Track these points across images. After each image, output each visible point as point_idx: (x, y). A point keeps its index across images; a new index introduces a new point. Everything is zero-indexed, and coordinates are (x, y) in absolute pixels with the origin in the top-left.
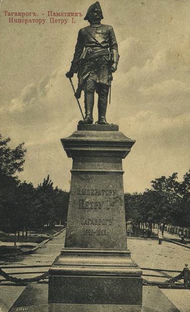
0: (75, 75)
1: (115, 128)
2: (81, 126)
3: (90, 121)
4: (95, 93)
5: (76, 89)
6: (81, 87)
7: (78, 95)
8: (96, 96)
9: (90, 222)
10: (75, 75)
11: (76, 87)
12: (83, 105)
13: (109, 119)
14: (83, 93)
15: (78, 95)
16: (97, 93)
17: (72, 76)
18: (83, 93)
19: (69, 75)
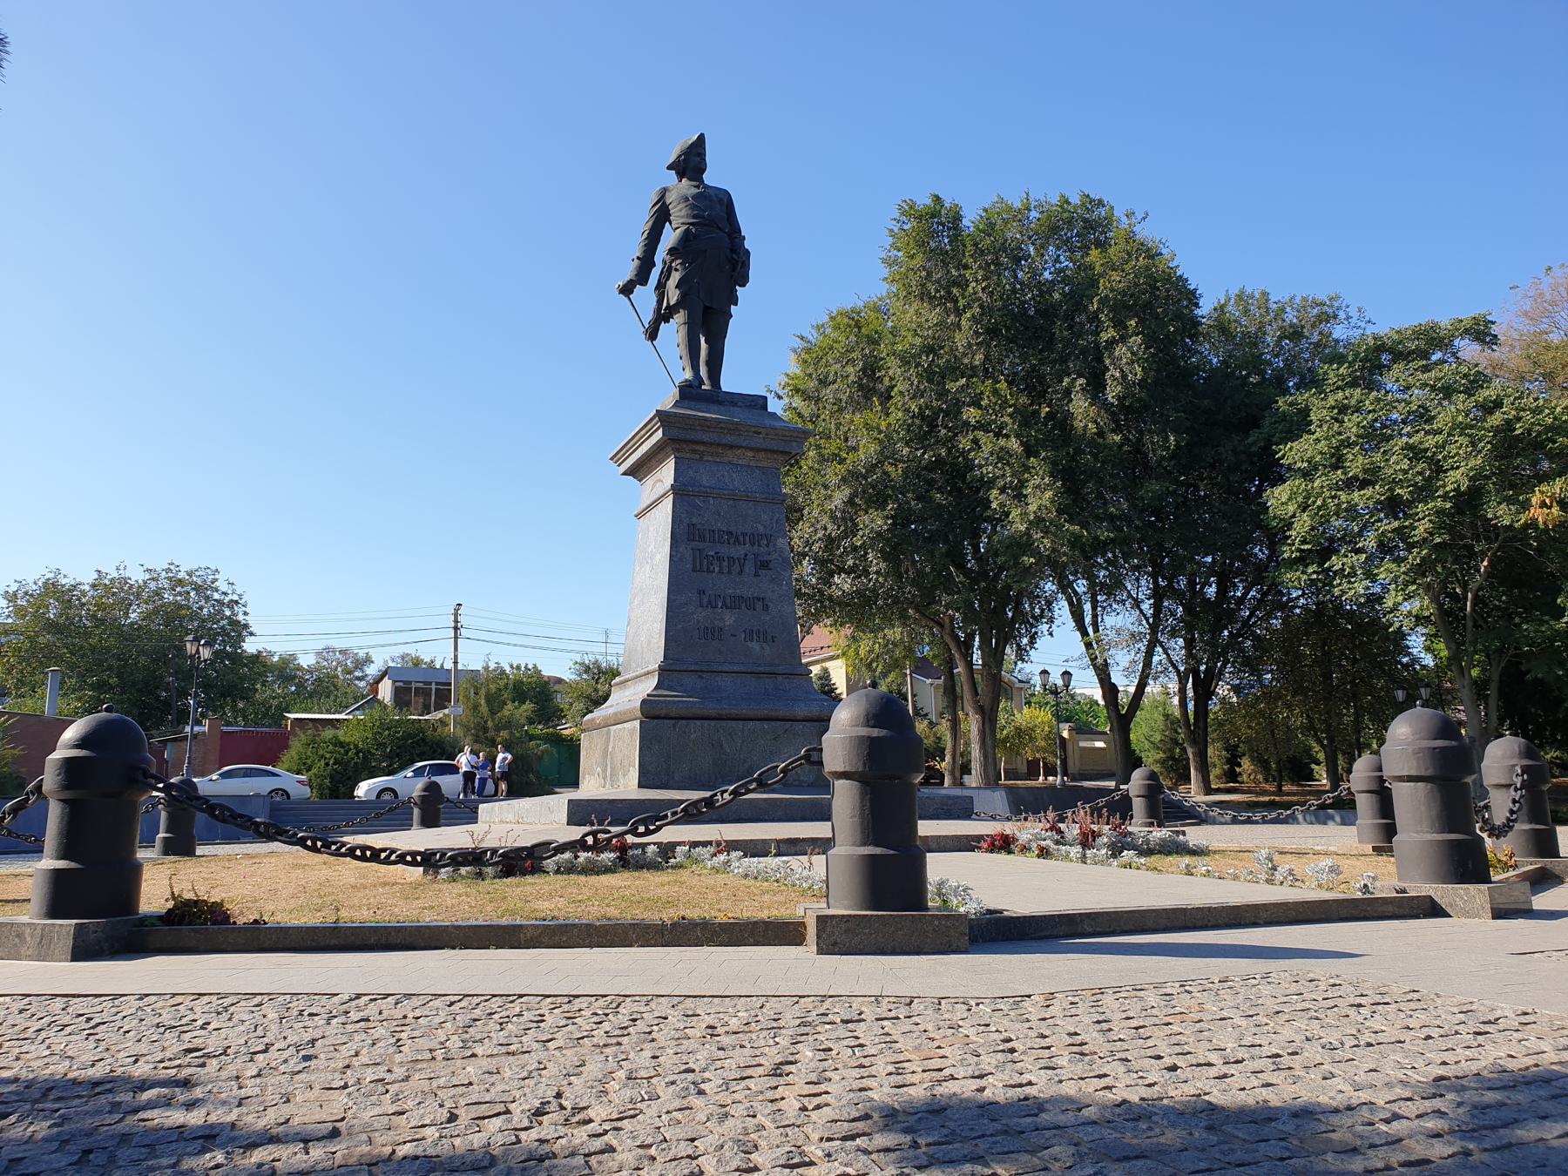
6: (663, 316)
9: (720, 605)
11: (648, 316)
15: (652, 334)
19: (627, 290)
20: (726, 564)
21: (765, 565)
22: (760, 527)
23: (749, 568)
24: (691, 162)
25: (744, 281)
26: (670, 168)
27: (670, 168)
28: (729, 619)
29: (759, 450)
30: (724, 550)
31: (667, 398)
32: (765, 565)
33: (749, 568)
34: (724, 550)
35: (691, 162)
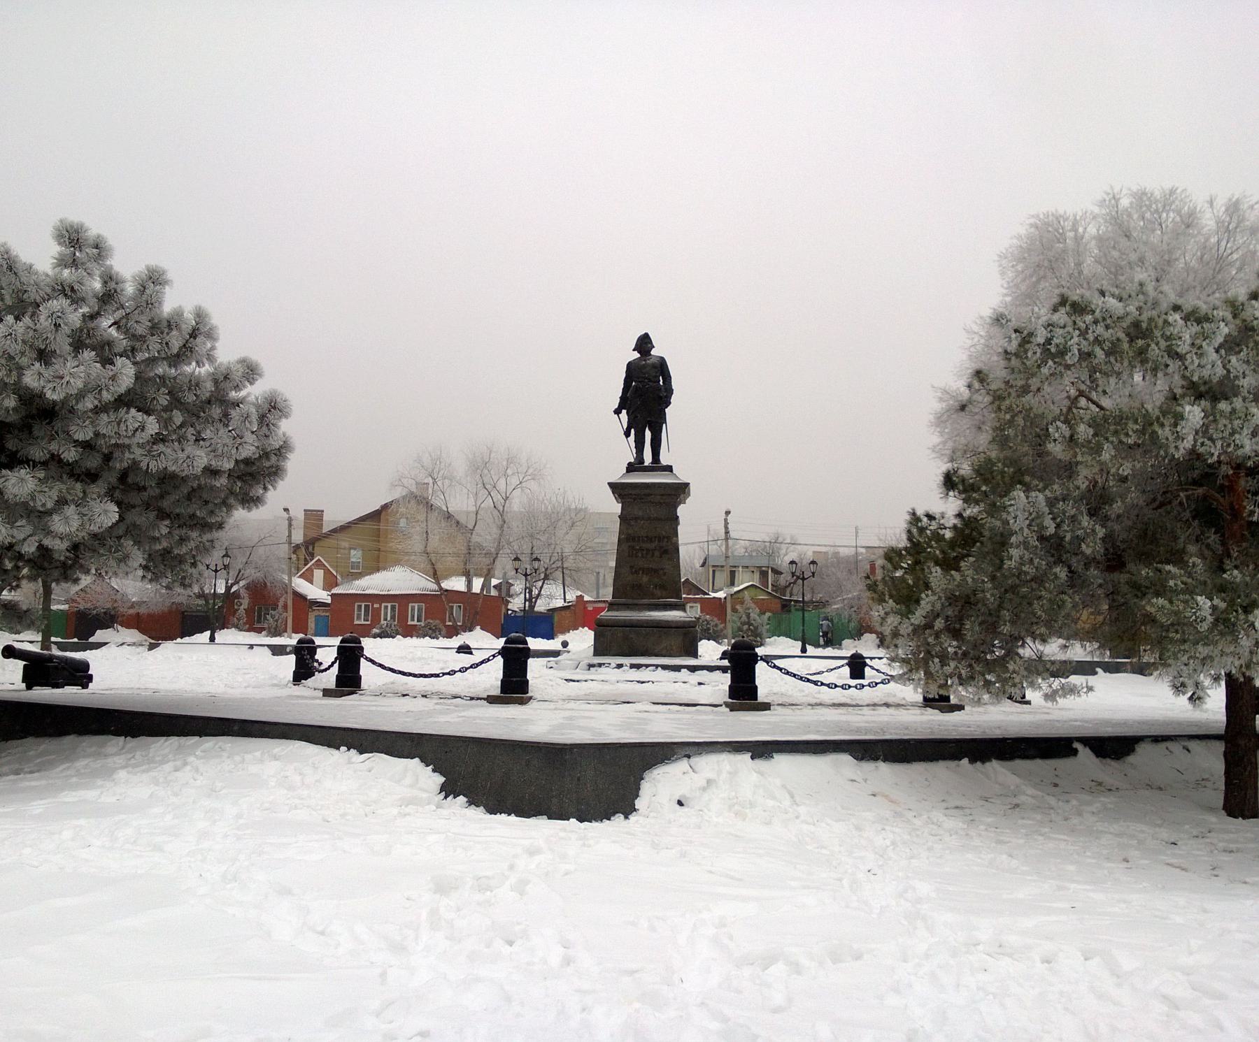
0: (624, 412)
1: (669, 469)
2: (631, 468)
3: (642, 461)
4: (647, 429)
5: (625, 427)
7: (627, 434)
8: (648, 434)
10: (624, 412)
11: (625, 427)
12: (633, 445)
13: (665, 459)
14: (633, 431)
16: (649, 429)
17: (621, 413)
18: (633, 431)
19: (617, 412)
20: (645, 552)
21: (666, 552)
22: (664, 533)
23: (657, 553)
24: (644, 344)
25: (668, 404)
26: (634, 350)
27: (634, 350)
28: (645, 579)
29: (662, 495)
30: (645, 546)
31: (618, 473)
32: (666, 552)
33: (657, 553)
34: (645, 546)
35: (644, 344)
